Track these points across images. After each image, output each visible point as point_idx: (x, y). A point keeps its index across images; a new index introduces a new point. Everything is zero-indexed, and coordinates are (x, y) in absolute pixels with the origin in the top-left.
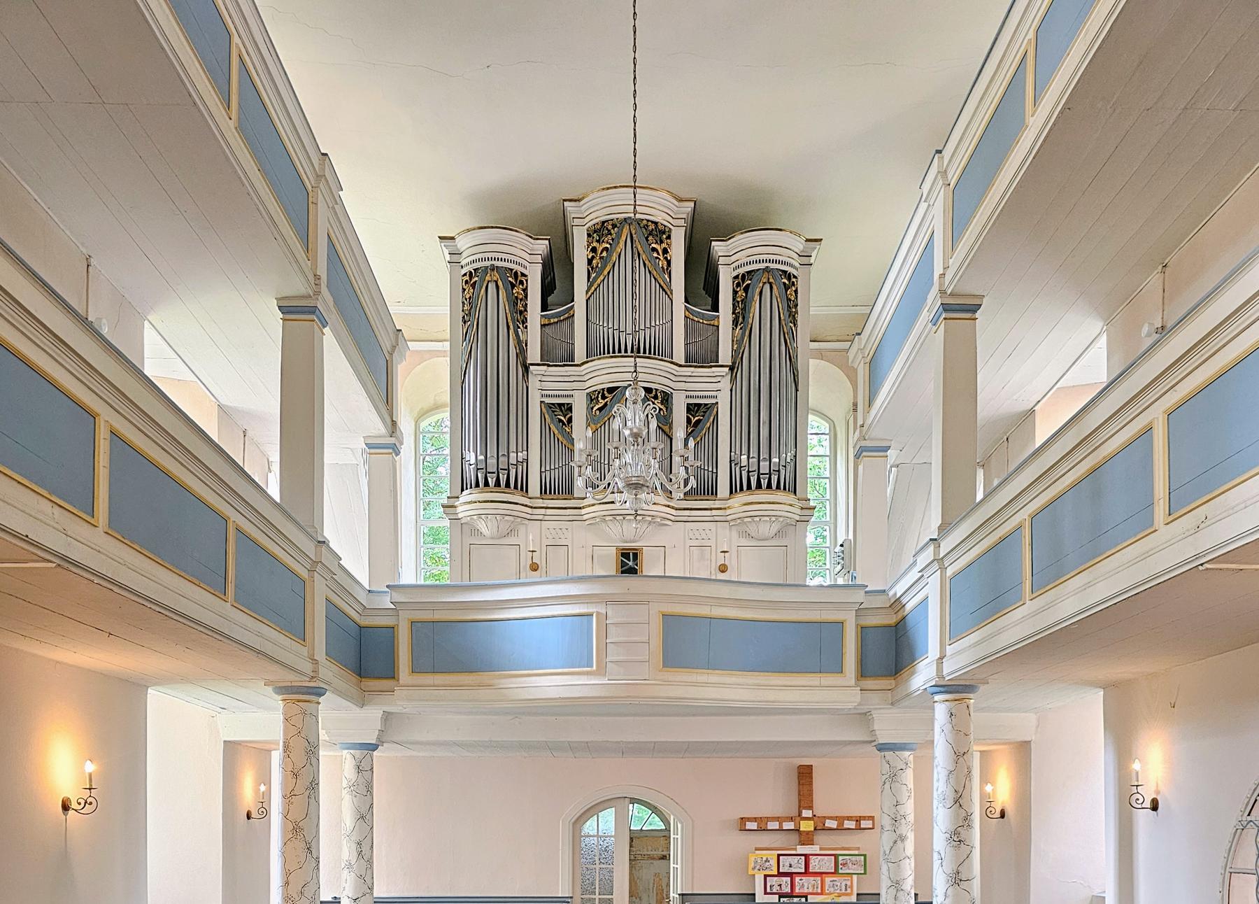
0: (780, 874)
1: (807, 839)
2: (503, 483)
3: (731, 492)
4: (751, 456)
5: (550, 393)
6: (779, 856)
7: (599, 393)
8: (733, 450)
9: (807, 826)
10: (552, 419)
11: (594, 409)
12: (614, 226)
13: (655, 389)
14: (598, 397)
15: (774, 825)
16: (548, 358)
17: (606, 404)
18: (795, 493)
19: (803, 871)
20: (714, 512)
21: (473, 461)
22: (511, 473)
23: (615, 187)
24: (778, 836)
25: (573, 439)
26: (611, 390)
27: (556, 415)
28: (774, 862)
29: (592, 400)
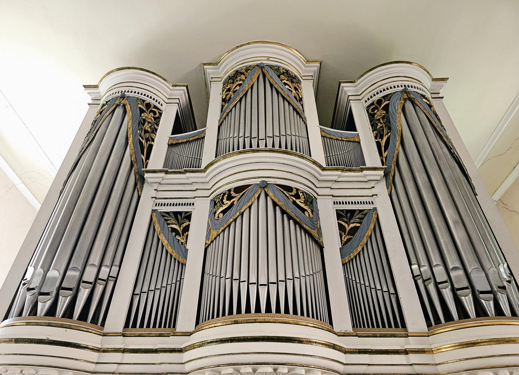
4: (451, 267)
5: (163, 201)
7: (224, 194)
8: (414, 261)
10: (163, 229)
11: (218, 213)
13: (296, 188)
14: (223, 199)
17: (232, 205)
22: (80, 295)
23: (248, 44)
25: (187, 250)
26: (238, 190)
27: (168, 224)
29: (215, 204)
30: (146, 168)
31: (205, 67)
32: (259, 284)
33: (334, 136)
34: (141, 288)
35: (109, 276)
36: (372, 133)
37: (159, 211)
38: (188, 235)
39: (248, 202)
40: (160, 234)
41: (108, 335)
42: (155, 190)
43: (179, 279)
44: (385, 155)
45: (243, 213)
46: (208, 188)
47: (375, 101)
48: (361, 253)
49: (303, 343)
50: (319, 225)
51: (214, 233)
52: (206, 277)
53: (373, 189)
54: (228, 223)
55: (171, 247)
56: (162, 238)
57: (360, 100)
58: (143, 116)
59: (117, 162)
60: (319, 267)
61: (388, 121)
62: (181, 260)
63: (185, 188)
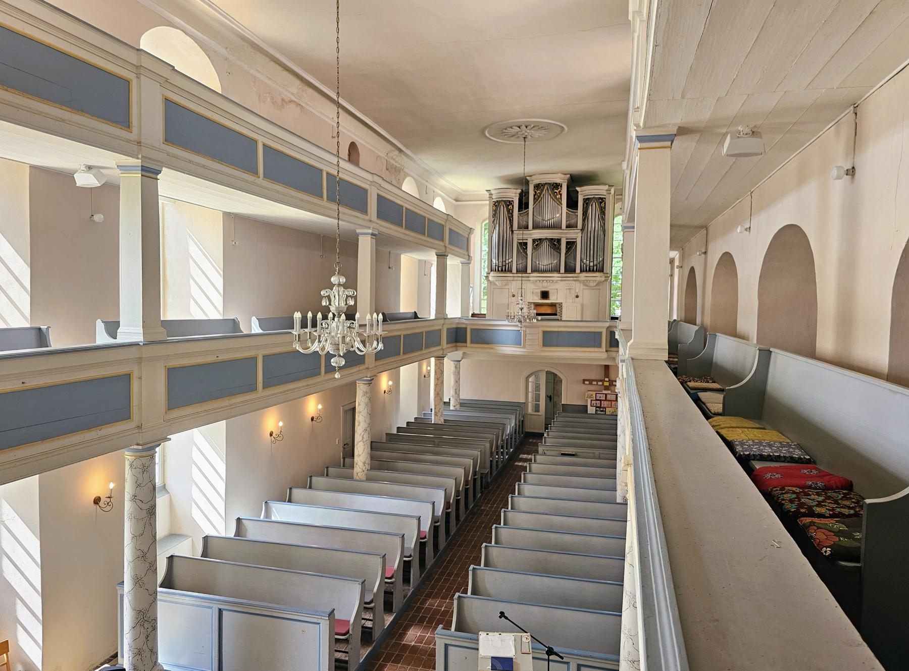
0: (596, 400)
1: (607, 388)
2: (504, 270)
3: (581, 271)
6: (596, 393)
9: (607, 384)
12: (542, 185)
15: (595, 383)
16: (519, 228)
18: (603, 271)
19: (604, 399)
20: (574, 278)
21: (494, 262)
24: (597, 386)
26: (540, 239)
28: (594, 396)
56: (521, 250)
60: (559, 258)
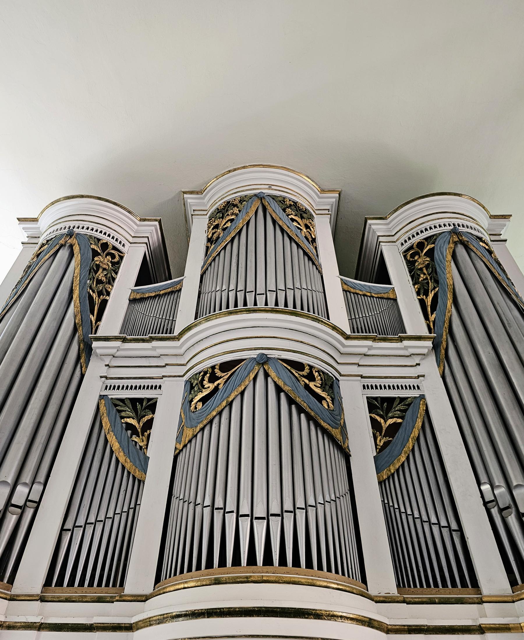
5: (117, 382)
7: (206, 373)
8: (483, 478)
10: (113, 425)
11: (195, 401)
13: (309, 365)
14: (203, 380)
17: (216, 389)
23: (244, 167)
25: (147, 459)
26: (226, 367)
29: (192, 387)
30: (95, 334)
31: (185, 196)
32: (254, 516)
33: (361, 290)
34: (74, 519)
35: (27, 500)
36: (412, 286)
37: (110, 397)
38: (150, 434)
39: (240, 385)
40: (108, 433)
41: (19, 598)
42: (107, 365)
43: (132, 505)
44: (432, 318)
45: (232, 402)
46: (182, 363)
47: (415, 244)
48: (406, 464)
49: (321, 619)
50: (343, 420)
51: (189, 433)
52: (174, 501)
53: (418, 366)
54: (210, 417)
55: (124, 453)
56: (112, 439)
57: (395, 242)
58: (97, 261)
59: (55, 324)
60: (344, 487)
61: (434, 271)
62: (138, 474)
63: (150, 363)
